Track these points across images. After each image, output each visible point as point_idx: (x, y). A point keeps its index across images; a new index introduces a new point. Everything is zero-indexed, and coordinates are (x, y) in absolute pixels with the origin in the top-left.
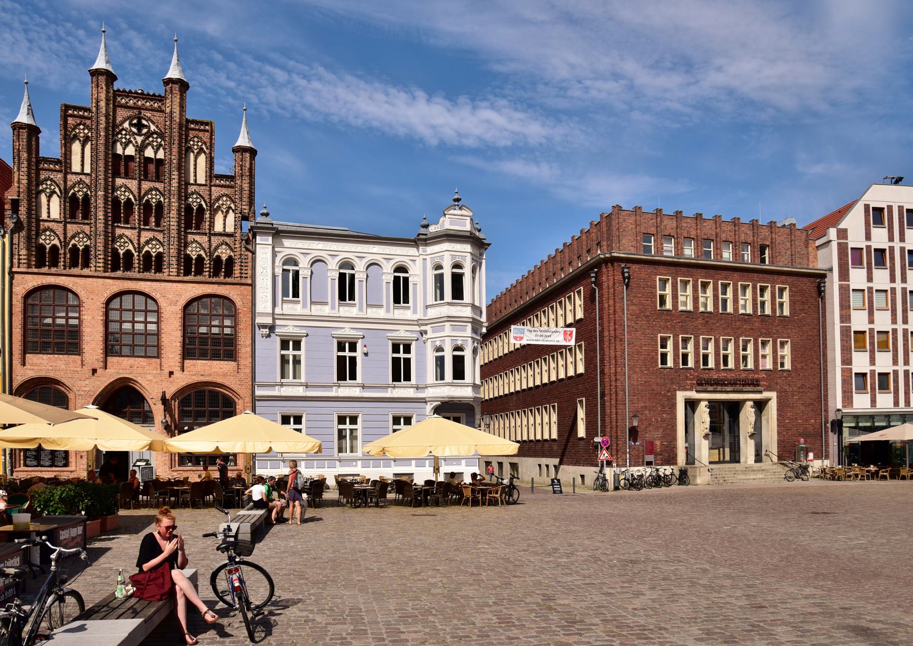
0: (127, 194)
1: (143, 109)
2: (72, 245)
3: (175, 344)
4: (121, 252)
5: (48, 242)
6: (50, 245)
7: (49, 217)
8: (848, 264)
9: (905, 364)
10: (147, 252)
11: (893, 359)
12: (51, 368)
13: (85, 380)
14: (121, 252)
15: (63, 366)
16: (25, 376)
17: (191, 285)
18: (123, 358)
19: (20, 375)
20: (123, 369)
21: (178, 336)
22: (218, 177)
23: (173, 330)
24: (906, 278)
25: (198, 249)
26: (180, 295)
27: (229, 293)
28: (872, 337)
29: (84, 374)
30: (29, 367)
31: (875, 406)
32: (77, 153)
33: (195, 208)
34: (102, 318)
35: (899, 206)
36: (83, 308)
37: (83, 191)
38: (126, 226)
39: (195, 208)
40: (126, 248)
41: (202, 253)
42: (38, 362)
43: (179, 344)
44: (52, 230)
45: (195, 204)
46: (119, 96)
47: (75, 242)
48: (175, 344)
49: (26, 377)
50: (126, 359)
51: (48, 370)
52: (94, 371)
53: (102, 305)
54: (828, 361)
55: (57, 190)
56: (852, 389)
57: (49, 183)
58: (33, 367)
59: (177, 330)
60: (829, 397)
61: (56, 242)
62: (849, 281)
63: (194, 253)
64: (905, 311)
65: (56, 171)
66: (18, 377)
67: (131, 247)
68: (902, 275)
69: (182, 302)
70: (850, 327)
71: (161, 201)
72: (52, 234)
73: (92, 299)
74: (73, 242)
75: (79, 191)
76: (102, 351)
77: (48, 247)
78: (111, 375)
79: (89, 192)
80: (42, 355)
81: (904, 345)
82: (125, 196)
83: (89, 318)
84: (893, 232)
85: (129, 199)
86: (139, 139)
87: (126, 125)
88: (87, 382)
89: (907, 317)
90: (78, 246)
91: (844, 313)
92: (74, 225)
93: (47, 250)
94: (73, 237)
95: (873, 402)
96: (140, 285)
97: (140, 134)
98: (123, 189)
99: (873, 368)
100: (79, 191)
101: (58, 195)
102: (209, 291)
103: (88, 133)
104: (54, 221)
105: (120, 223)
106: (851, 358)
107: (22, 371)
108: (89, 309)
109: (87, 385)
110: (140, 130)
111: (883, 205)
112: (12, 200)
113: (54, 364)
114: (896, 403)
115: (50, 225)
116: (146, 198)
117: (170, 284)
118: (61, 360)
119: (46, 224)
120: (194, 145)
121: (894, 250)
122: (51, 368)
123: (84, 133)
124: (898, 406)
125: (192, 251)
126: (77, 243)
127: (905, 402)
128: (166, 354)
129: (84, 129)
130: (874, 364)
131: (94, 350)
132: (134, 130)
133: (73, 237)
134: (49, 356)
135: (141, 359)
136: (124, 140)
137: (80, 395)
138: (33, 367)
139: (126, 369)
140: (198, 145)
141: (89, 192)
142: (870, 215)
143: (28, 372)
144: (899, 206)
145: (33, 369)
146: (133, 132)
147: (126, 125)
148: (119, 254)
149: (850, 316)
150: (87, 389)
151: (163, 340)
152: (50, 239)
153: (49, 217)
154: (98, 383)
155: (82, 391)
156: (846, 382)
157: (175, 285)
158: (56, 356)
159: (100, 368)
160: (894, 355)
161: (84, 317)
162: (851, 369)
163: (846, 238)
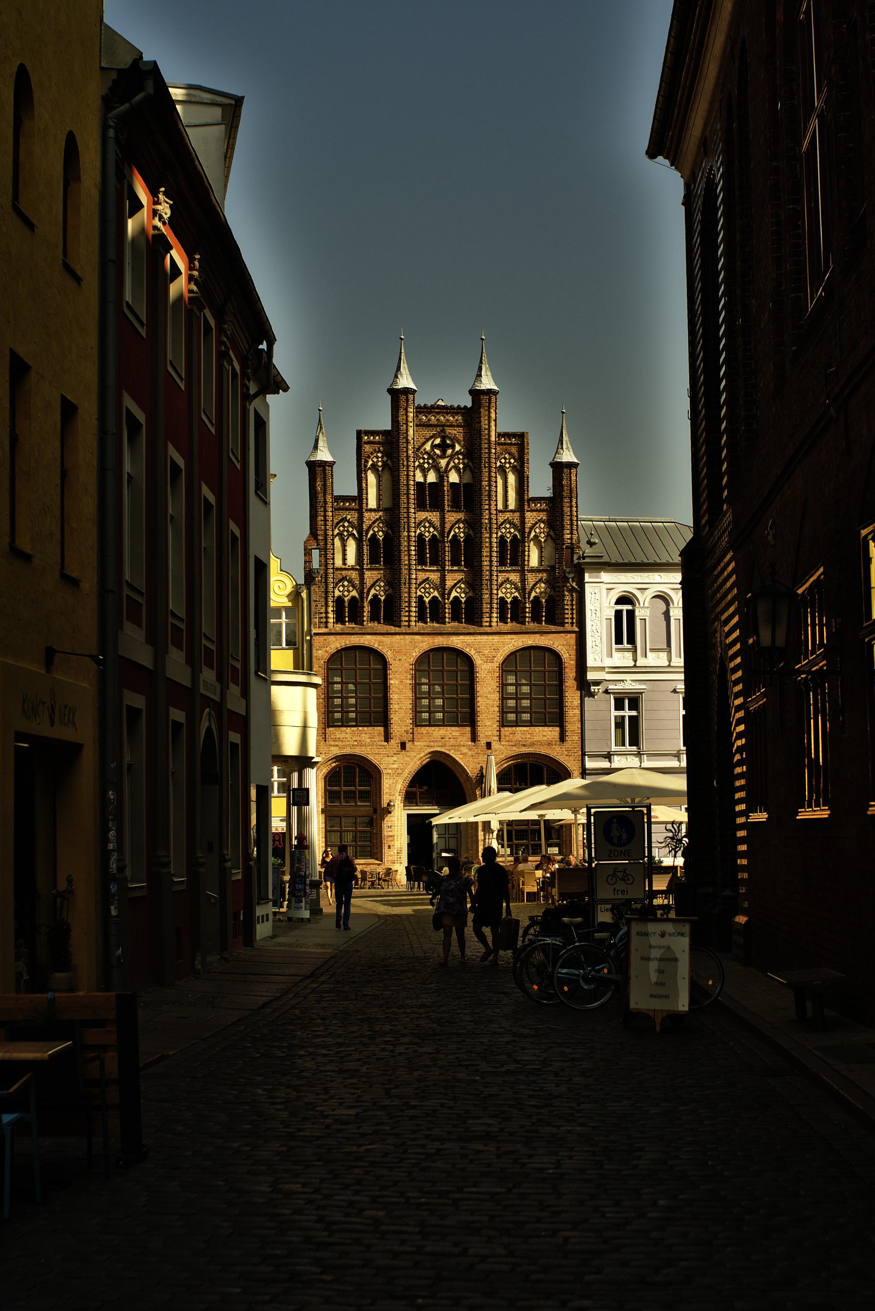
0: (432, 530)
1: (448, 426)
2: (373, 596)
3: (492, 709)
4: (427, 600)
5: (346, 593)
6: (349, 597)
7: (344, 564)
10: (456, 598)
12: (356, 743)
13: (393, 756)
14: (427, 600)
15: (368, 740)
17: (509, 636)
18: (433, 728)
19: (323, 752)
20: (433, 741)
21: (495, 700)
22: (535, 500)
23: (490, 693)
25: (514, 590)
26: (497, 650)
27: (553, 644)
29: (392, 748)
30: (333, 743)
33: (509, 540)
34: (411, 682)
36: (390, 671)
38: (432, 568)
39: (509, 540)
40: (432, 596)
41: (517, 594)
43: (497, 709)
44: (350, 581)
45: (508, 535)
46: (420, 413)
47: (375, 592)
48: (492, 709)
49: (330, 755)
50: (437, 728)
51: (353, 746)
52: (403, 746)
53: (411, 667)
55: (355, 532)
58: (337, 743)
59: (494, 692)
61: (354, 593)
63: (508, 595)
67: (436, 594)
69: (500, 658)
71: (470, 535)
73: (400, 660)
75: (378, 532)
76: (411, 721)
77: (346, 599)
78: (421, 749)
79: (390, 531)
80: (344, 729)
82: (429, 532)
83: (397, 682)
85: (434, 535)
86: (443, 462)
87: (428, 447)
88: (395, 758)
92: (375, 572)
93: (346, 604)
96: (452, 640)
97: (443, 456)
98: (427, 525)
100: (378, 532)
102: (530, 642)
103: (387, 461)
105: (426, 566)
108: (397, 672)
109: (394, 761)
110: (444, 452)
113: (359, 738)
116: (452, 533)
117: (486, 637)
118: (366, 733)
119: (344, 573)
120: (505, 463)
122: (356, 743)
125: (506, 593)
126: (378, 593)
128: (482, 721)
131: (402, 720)
132: (438, 452)
134: (352, 728)
135: (453, 728)
136: (426, 466)
137: (388, 774)
138: (337, 743)
139: (437, 741)
140: (510, 463)
141: (390, 531)
143: (332, 748)
145: (337, 746)
146: (438, 455)
147: (428, 447)
148: (424, 602)
150: (394, 766)
151: (479, 704)
152: (348, 591)
153: (344, 564)
154: (407, 759)
155: (389, 769)
157: (490, 637)
158: (360, 728)
159: (409, 741)
161: (392, 682)
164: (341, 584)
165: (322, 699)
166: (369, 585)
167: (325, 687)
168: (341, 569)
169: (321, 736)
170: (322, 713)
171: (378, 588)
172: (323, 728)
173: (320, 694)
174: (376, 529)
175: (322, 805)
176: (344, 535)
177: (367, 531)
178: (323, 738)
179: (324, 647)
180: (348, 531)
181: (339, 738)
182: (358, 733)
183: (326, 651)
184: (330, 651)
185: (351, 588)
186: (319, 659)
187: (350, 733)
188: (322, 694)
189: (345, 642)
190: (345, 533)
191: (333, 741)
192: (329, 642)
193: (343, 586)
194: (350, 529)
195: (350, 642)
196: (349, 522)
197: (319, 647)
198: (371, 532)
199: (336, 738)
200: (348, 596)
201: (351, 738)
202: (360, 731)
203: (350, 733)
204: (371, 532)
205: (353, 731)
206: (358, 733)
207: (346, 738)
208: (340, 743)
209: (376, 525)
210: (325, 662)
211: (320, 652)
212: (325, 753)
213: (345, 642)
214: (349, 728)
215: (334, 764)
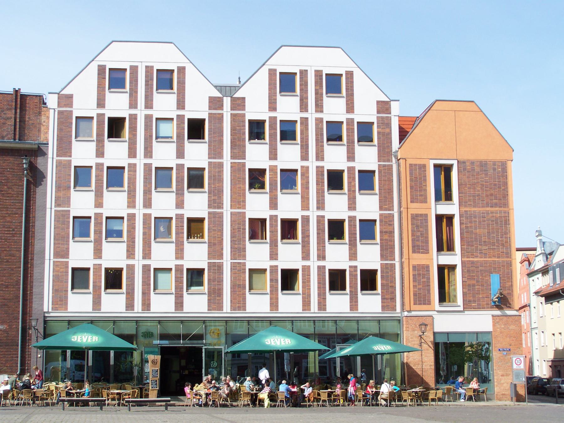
8: (71, 136)
9: (144, 258)
11: (128, 251)
24: (151, 152)
28: (98, 224)
31: (100, 310)
35: (147, 67)
54: (35, 252)
56: (67, 287)
60: (34, 297)
62: (70, 156)
64: (147, 192)
68: (146, 148)
70: (69, 211)
81: (144, 234)
84: (136, 97)
89: (150, 199)
91: (61, 194)
95: (97, 303)
99: (98, 262)
106: (68, 249)
111: (126, 66)
114: (130, 305)
121: (136, 119)
124: (133, 310)
127: (143, 305)
130: (100, 257)
142: (105, 78)
144: (147, 67)
149: (69, 198)
156: (58, 279)
160: (128, 246)
162: (67, 262)
163: (71, 105)
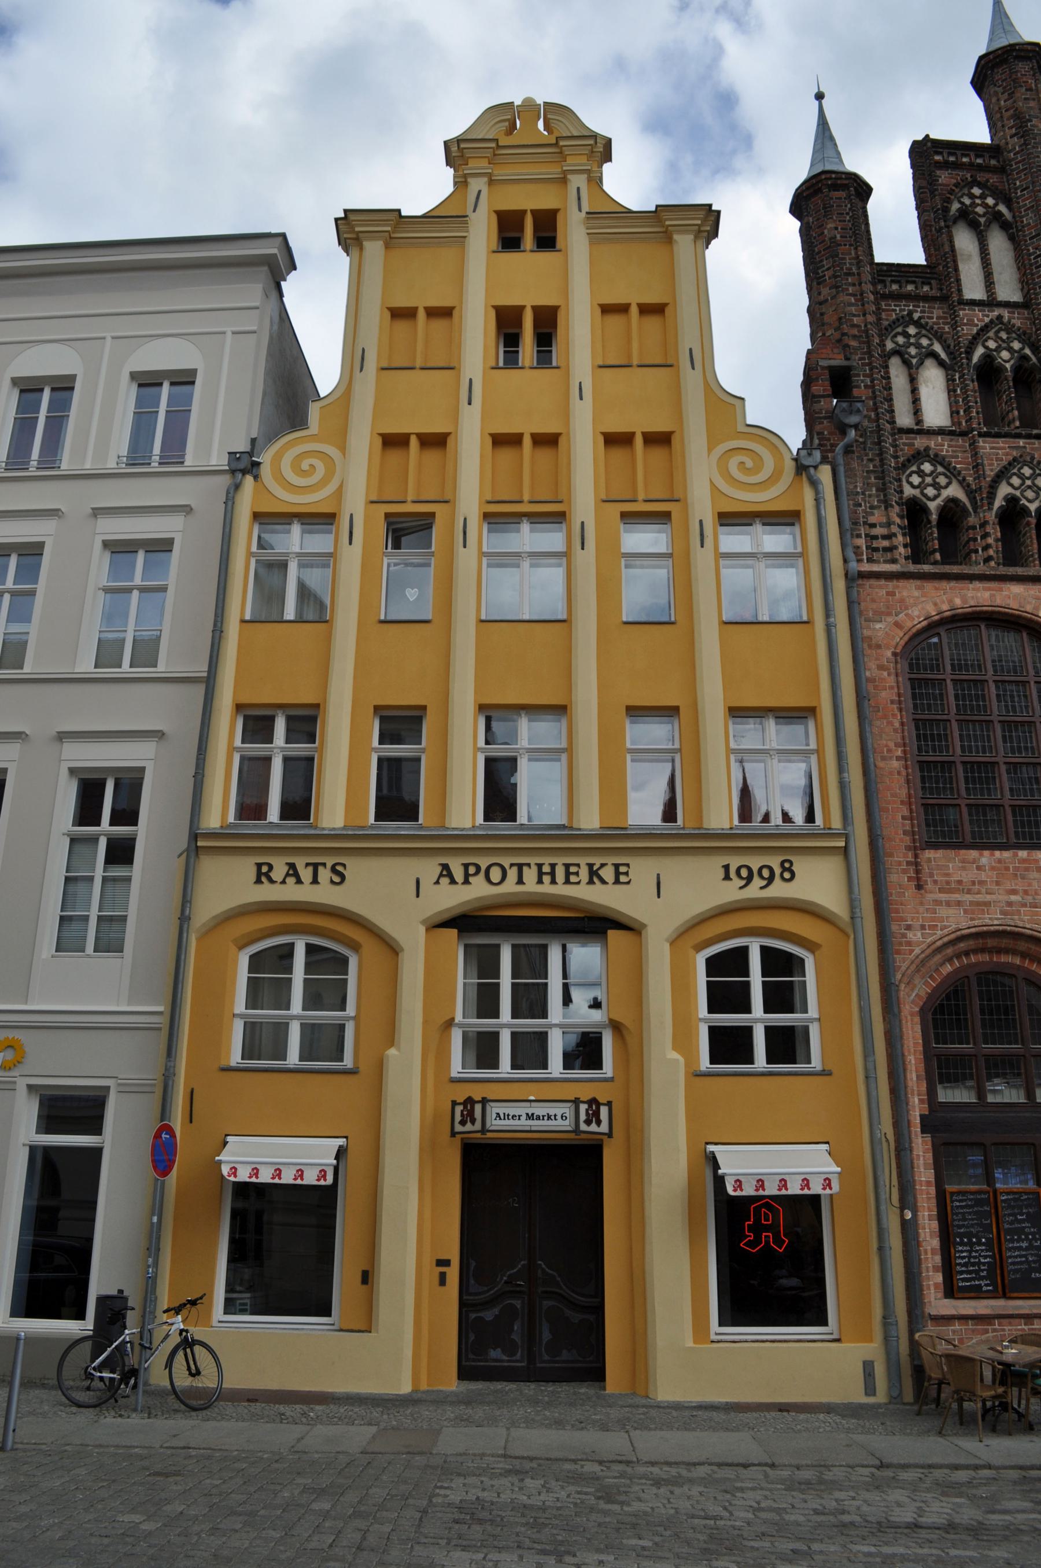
5: (930, 491)
6: (939, 501)
16: (933, 927)
32: (970, 256)
37: (1010, 349)
42: (967, 876)
44: (937, 460)
49: (939, 932)
55: (937, 348)
57: (912, 330)
61: (954, 491)
65: (926, 298)
66: (910, 935)
72: (940, 469)
74: (1004, 490)
75: (998, 349)
77: (933, 506)
79: (1027, 351)
80: (974, 854)
90: (1024, 501)
94: (1003, 475)
100: (998, 349)
101: (941, 363)
103: (996, 205)
104: (941, 431)
107: (921, 909)
112: (831, 369)
115: (932, 443)
119: (920, 442)
123: (986, 206)
126: (1018, 493)
129: (983, 197)
133: (1003, 475)
134: (997, 853)
138: (957, 897)
143: (943, 912)
152: (936, 486)
158: (1023, 854)
164: (914, 468)
165: (898, 758)
166: (990, 473)
167: (902, 724)
168: (909, 431)
169: (904, 871)
170: (902, 803)
171: (1016, 481)
172: (908, 848)
173: (892, 745)
174: (992, 345)
175: (921, 1101)
176: (909, 354)
177: (969, 352)
178: (910, 879)
179: (889, 614)
180: (918, 346)
181: (960, 882)
182: (1016, 869)
183: (897, 624)
184: (909, 624)
185: (942, 480)
186: (879, 647)
187: (993, 868)
188: (897, 745)
189: (950, 601)
190: (913, 351)
191: (941, 890)
192: (902, 601)
193: (921, 473)
194: (925, 342)
195: (964, 599)
196: (917, 324)
197: (875, 612)
198: (980, 351)
199: (948, 883)
200: (936, 497)
201: (998, 883)
202: (1024, 861)
203: (993, 868)
204: (980, 351)
205: (1000, 861)
206: (1016, 869)
207: (982, 883)
208: (968, 898)
209: (991, 334)
210: (895, 654)
211: (878, 626)
212: (923, 927)
213: (950, 601)
214: (986, 853)
215: (948, 968)
